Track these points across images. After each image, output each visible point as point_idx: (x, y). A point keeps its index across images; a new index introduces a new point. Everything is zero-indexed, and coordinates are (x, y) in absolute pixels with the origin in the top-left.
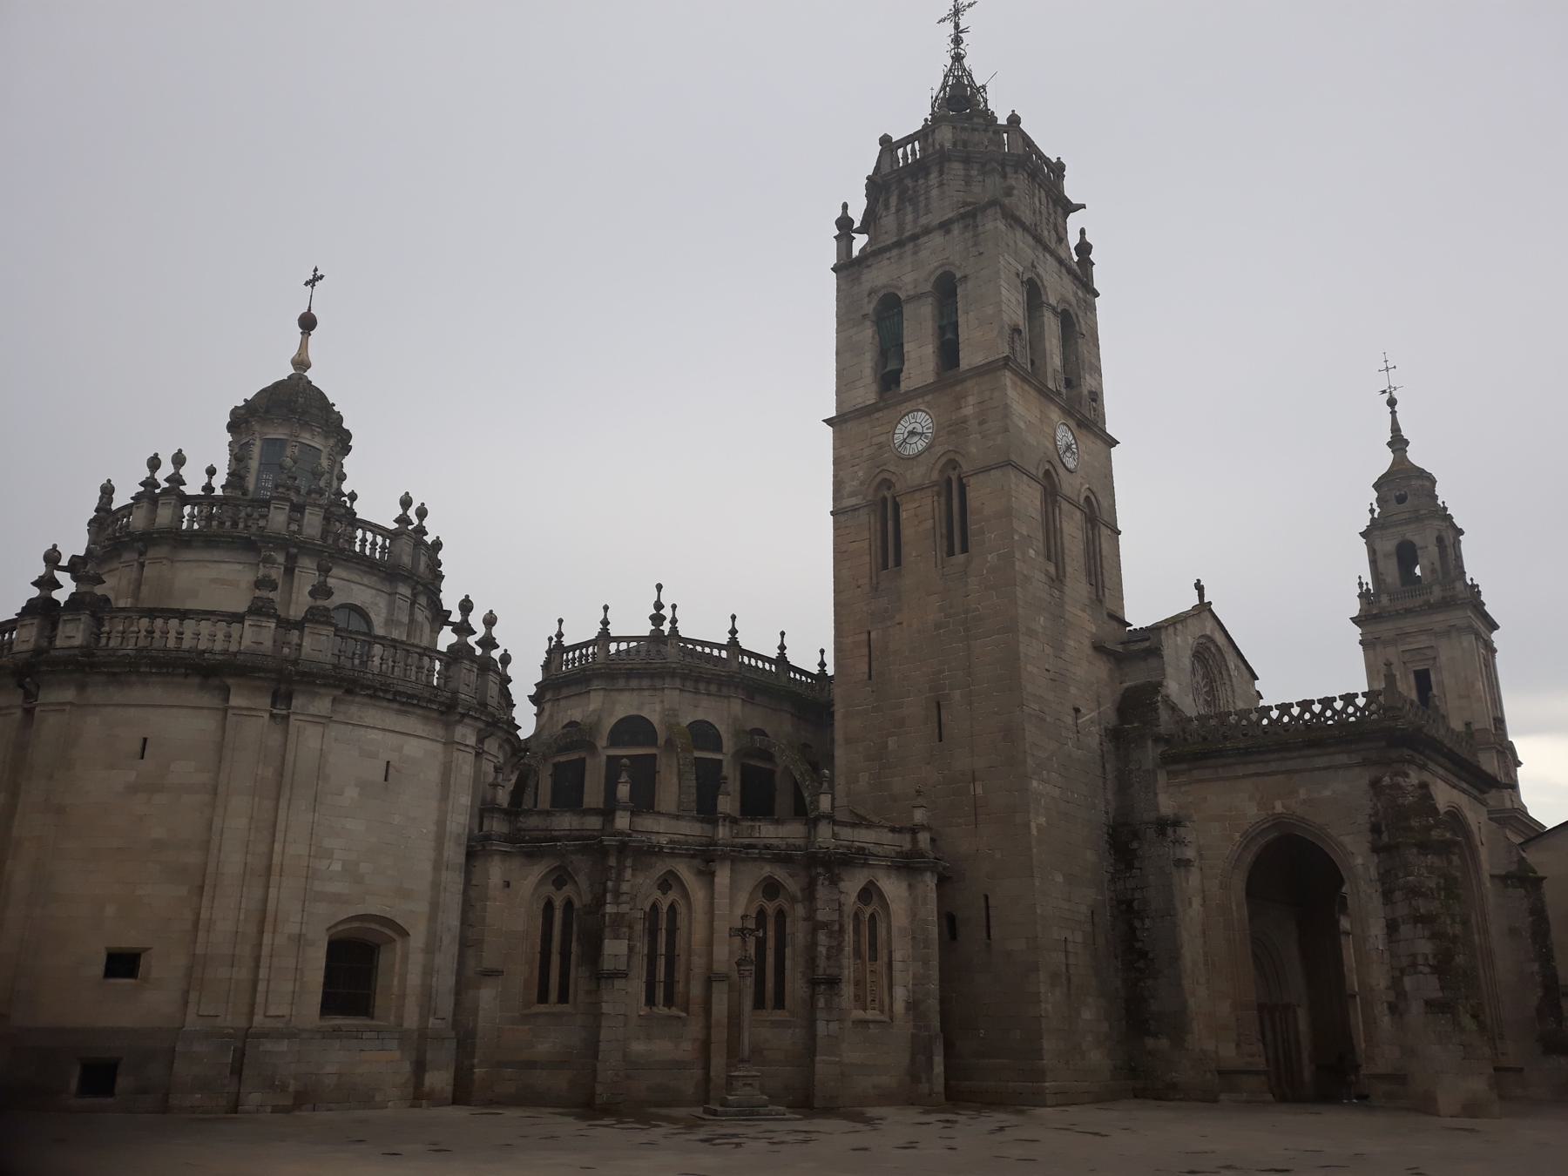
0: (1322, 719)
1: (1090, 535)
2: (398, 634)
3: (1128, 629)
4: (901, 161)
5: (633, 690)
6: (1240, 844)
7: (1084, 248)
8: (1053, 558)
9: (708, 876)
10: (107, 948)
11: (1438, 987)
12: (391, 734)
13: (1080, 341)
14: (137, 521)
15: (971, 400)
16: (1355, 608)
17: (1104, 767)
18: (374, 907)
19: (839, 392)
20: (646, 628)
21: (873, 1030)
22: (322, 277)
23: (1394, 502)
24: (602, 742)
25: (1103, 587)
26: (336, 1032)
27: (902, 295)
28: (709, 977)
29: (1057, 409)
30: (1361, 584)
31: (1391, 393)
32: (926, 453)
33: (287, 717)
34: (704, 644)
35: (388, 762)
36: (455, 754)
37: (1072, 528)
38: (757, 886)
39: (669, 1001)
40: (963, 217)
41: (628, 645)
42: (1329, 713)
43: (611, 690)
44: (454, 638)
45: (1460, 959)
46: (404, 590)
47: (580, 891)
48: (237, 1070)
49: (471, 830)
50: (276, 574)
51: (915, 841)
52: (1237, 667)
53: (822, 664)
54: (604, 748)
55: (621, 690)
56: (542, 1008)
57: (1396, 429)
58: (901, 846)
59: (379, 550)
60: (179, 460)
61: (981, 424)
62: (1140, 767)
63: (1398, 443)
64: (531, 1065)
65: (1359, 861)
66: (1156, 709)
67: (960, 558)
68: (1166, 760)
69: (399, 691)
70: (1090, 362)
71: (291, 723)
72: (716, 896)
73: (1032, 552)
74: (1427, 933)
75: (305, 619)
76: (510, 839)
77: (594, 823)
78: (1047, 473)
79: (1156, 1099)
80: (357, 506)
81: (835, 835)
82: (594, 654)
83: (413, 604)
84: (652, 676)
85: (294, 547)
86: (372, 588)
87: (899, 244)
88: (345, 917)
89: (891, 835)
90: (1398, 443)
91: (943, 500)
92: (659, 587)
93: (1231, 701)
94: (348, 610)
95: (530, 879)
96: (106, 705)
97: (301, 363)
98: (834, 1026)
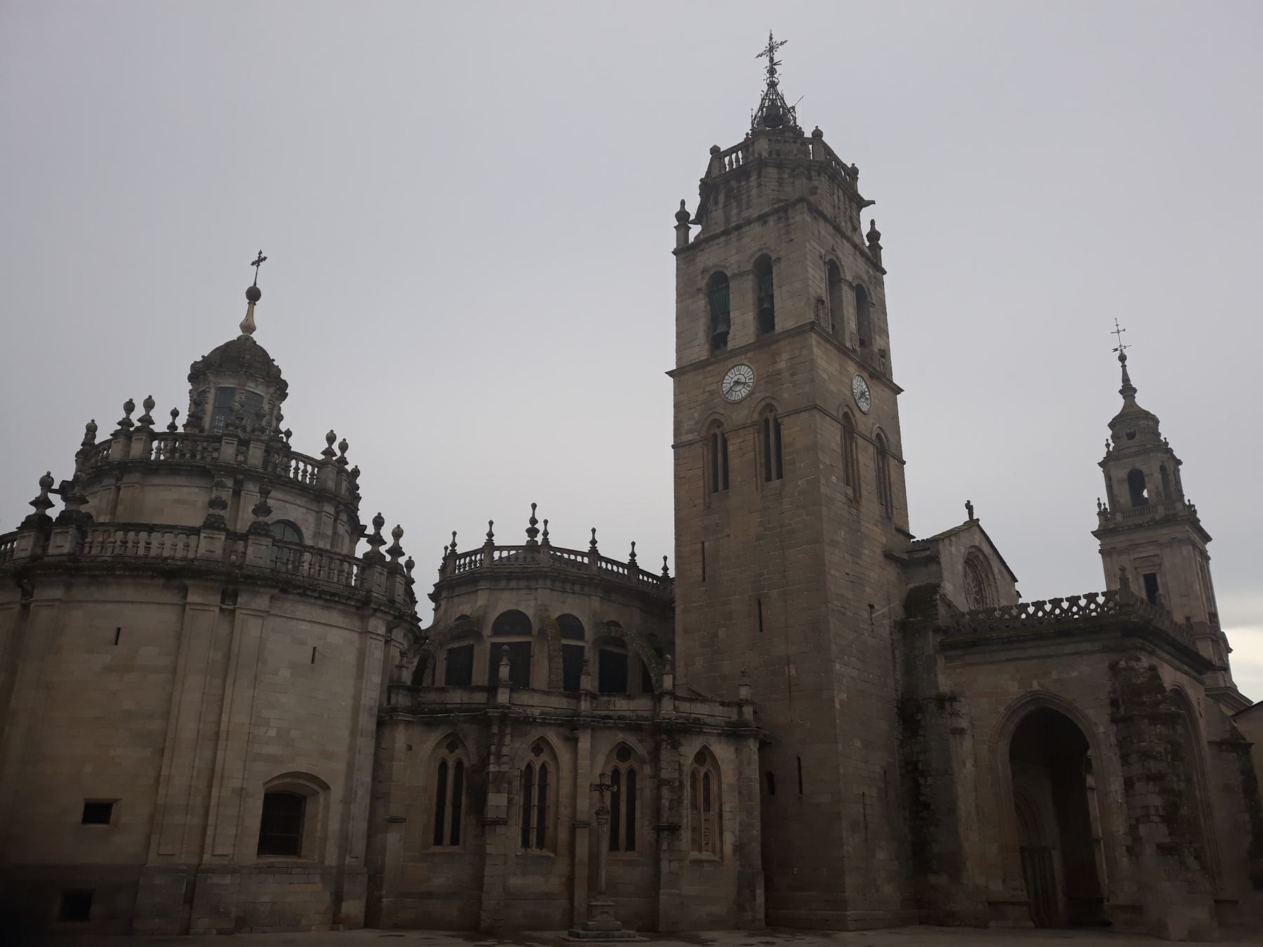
0: (1070, 614)
1: (881, 465)
2: (324, 544)
3: (912, 540)
4: (727, 166)
5: (512, 589)
6: (1005, 716)
7: (874, 236)
8: (851, 484)
9: (573, 741)
10: (85, 799)
11: (1167, 833)
12: (316, 625)
13: (871, 309)
14: (115, 453)
15: (785, 356)
16: (1095, 524)
17: (893, 652)
18: (301, 765)
19: (678, 350)
20: (523, 540)
22: (265, 258)
23: (1126, 438)
24: (487, 631)
25: (892, 506)
26: (270, 869)
27: (728, 273)
28: (574, 825)
29: (852, 363)
30: (1099, 505)
31: (1121, 350)
32: (748, 399)
33: (233, 612)
34: (570, 552)
35: (315, 648)
36: (369, 643)
37: (866, 459)
38: (613, 748)
39: (541, 844)
40: (777, 211)
41: (509, 553)
42: (1075, 609)
43: (494, 589)
44: (368, 548)
45: (1184, 811)
46: (329, 509)
47: (469, 754)
48: (189, 900)
49: (381, 704)
50: (226, 495)
51: (740, 713)
52: (1000, 571)
53: (665, 569)
54: (488, 637)
55: (503, 589)
56: (438, 849)
57: (1126, 379)
58: (730, 718)
59: (309, 476)
60: (149, 404)
61: (792, 375)
62: (923, 653)
63: (1128, 390)
64: (429, 895)
65: (1101, 729)
66: (935, 606)
67: (776, 483)
68: (944, 648)
69: (324, 591)
70: (879, 326)
71: (237, 616)
72: (579, 758)
73: (834, 479)
74: (1157, 789)
75: (249, 532)
76: (412, 711)
77: (480, 698)
78: (846, 415)
79: (937, 925)
80: (291, 441)
81: (675, 708)
82: (481, 560)
83: (335, 520)
84: (528, 578)
85: (241, 474)
86: (303, 507)
87: (726, 233)
88: (279, 774)
89: (721, 708)
90: (1128, 390)
91: (762, 436)
92: (534, 506)
93: (995, 599)
94: (283, 525)
95: (428, 743)
96: (88, 602)
97: (248, 327)
98: (675, 865)
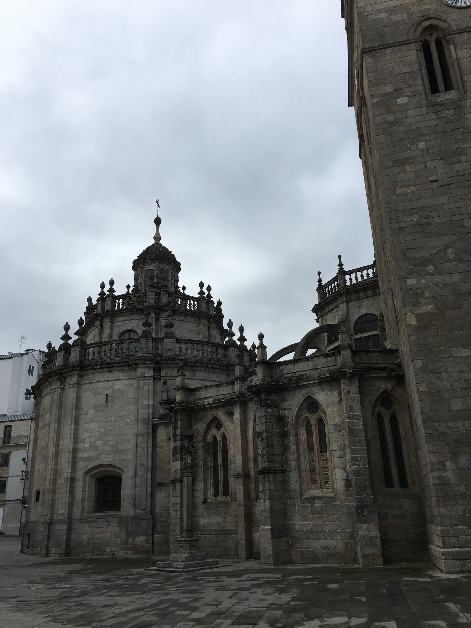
18: (104, 460)
21: (318, 504)
35: (107, 395)
97: (157, 238)
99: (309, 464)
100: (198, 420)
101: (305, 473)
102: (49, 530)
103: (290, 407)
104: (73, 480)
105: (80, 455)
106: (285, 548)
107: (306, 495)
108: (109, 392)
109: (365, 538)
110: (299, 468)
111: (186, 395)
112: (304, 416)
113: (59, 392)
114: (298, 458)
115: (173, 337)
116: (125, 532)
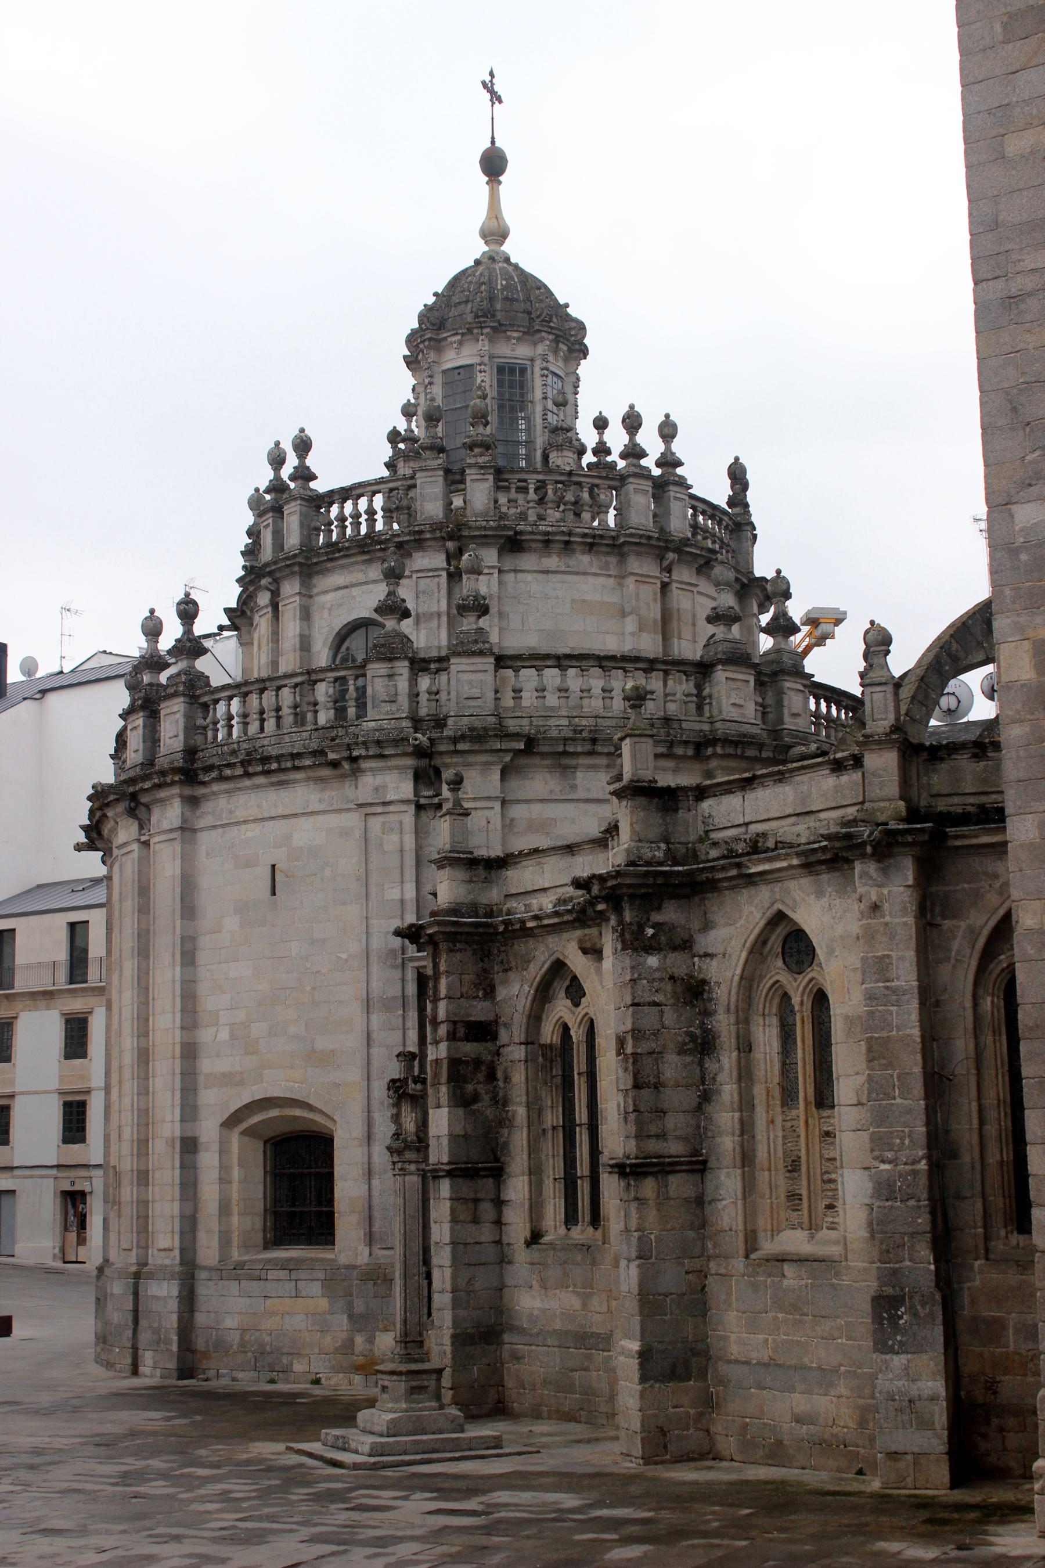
12: (271, 823)
21: (792, 1277)
35: (273, 866)
99: (784, 1144)
100: (510, 969)
101: (766, 1173)
102: (136, 1294)
103: (722, 950)
104: (189, 1146)
105: (207, 1065)
106: (692, 1411)
107: (768, 1247)
108: (278, 856)
109: (893, 1400)
110: (746, 1158)
111: (471, 881)
112: (771, 982)
113: (135, 855)
114: (746, 1128)
115: (481, 653)
116: (345, 1316)
